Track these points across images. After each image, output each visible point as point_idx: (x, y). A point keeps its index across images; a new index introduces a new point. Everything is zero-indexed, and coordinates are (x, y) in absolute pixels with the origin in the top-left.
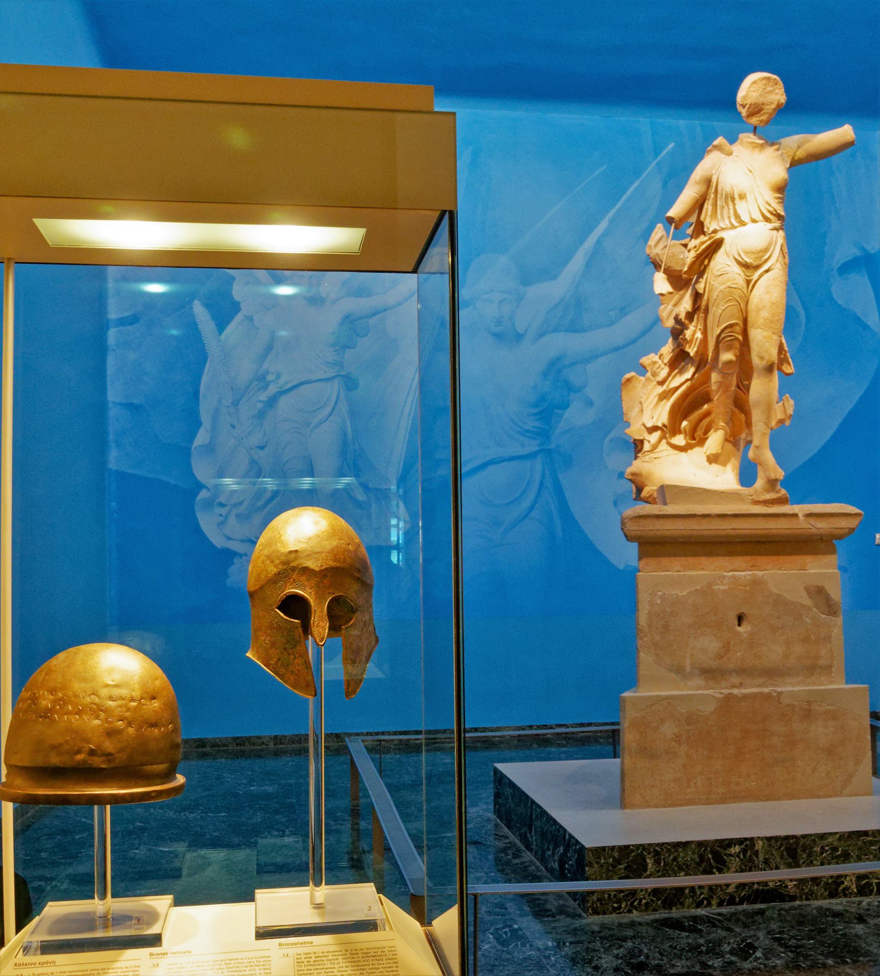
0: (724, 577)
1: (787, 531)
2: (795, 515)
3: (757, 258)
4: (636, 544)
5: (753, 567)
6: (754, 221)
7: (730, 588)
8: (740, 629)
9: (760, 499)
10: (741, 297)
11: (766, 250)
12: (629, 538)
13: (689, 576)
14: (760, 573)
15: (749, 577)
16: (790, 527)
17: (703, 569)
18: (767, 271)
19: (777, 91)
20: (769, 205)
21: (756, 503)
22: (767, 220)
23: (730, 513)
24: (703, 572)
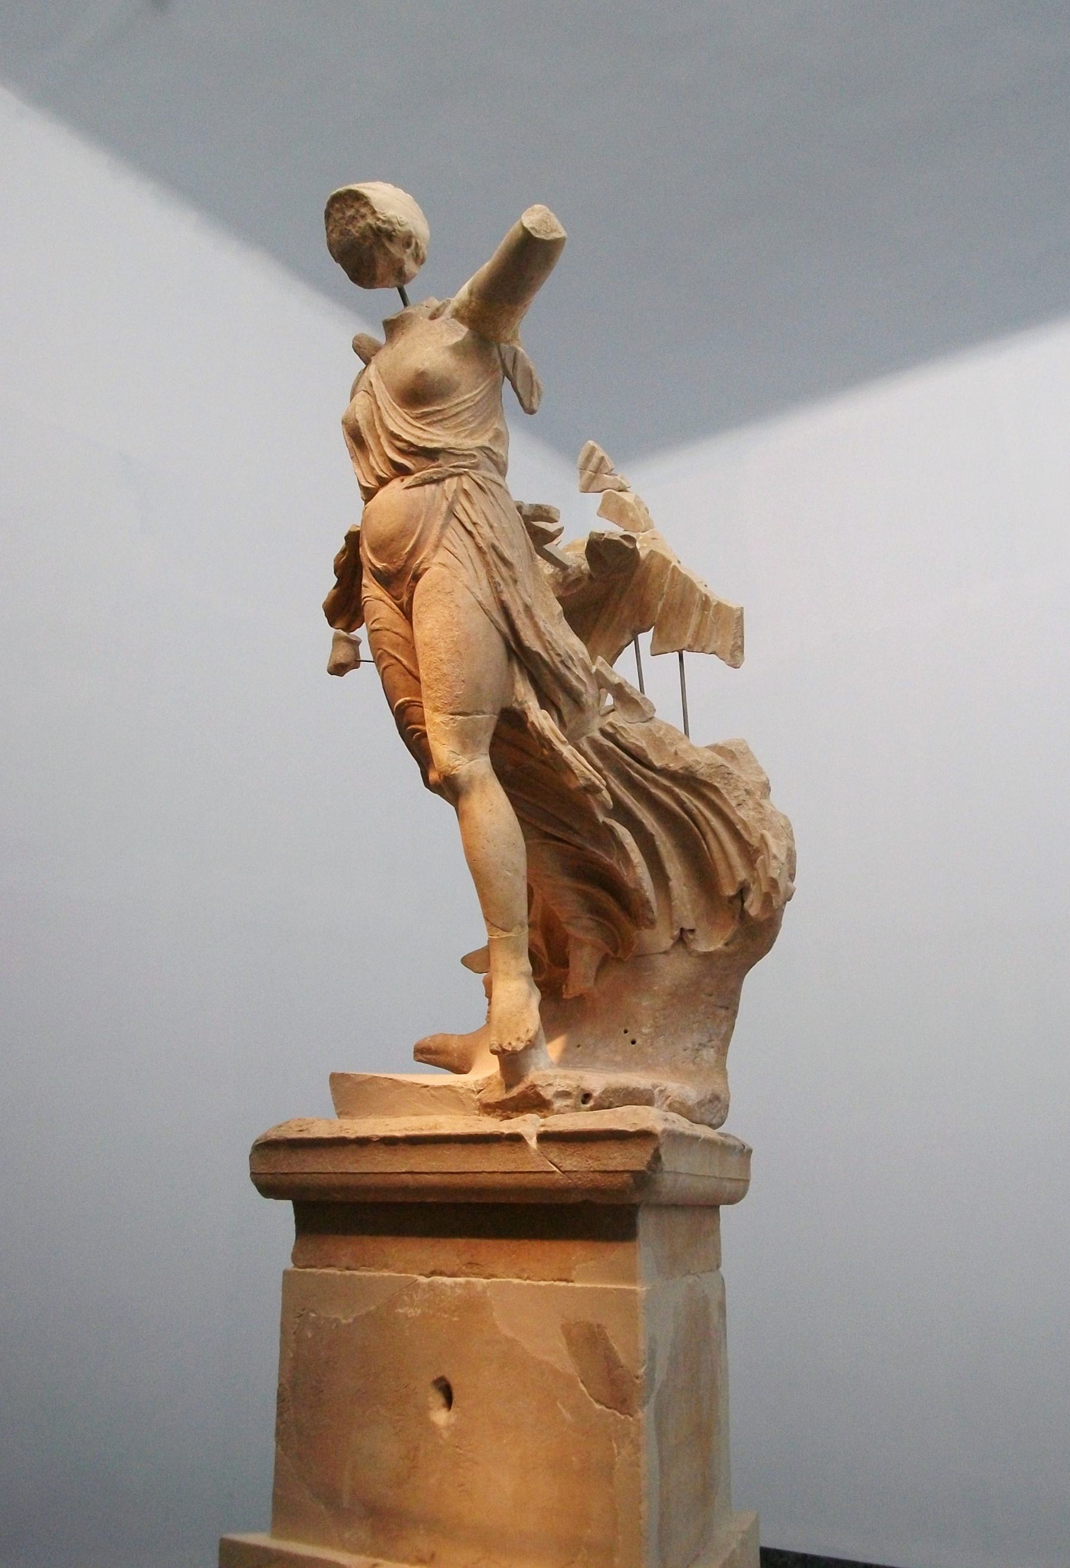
0: (415, 1285)
1: (509, 1180)
2: (517, 1139)
3: (391, 556)
4: (289, 1204)
5: (473, 1267)
6: (383, 482)
7: (423, 1313)
8: (441, 1417)
9: (492, 1101)
10: (396, 646)
11: (404, 533)
12: (269, 1189)
13: (360, 1279)
14: (480, 1282)
15: (459, 1291)
16: (511, 1167)
17: (386, 1266)
18: (416, 578)
19: (363, 210)
20: (398, 438)
21: (488, 1108)
22: (402, 471)
23: (398, 1134)
24: (386, 1273)
